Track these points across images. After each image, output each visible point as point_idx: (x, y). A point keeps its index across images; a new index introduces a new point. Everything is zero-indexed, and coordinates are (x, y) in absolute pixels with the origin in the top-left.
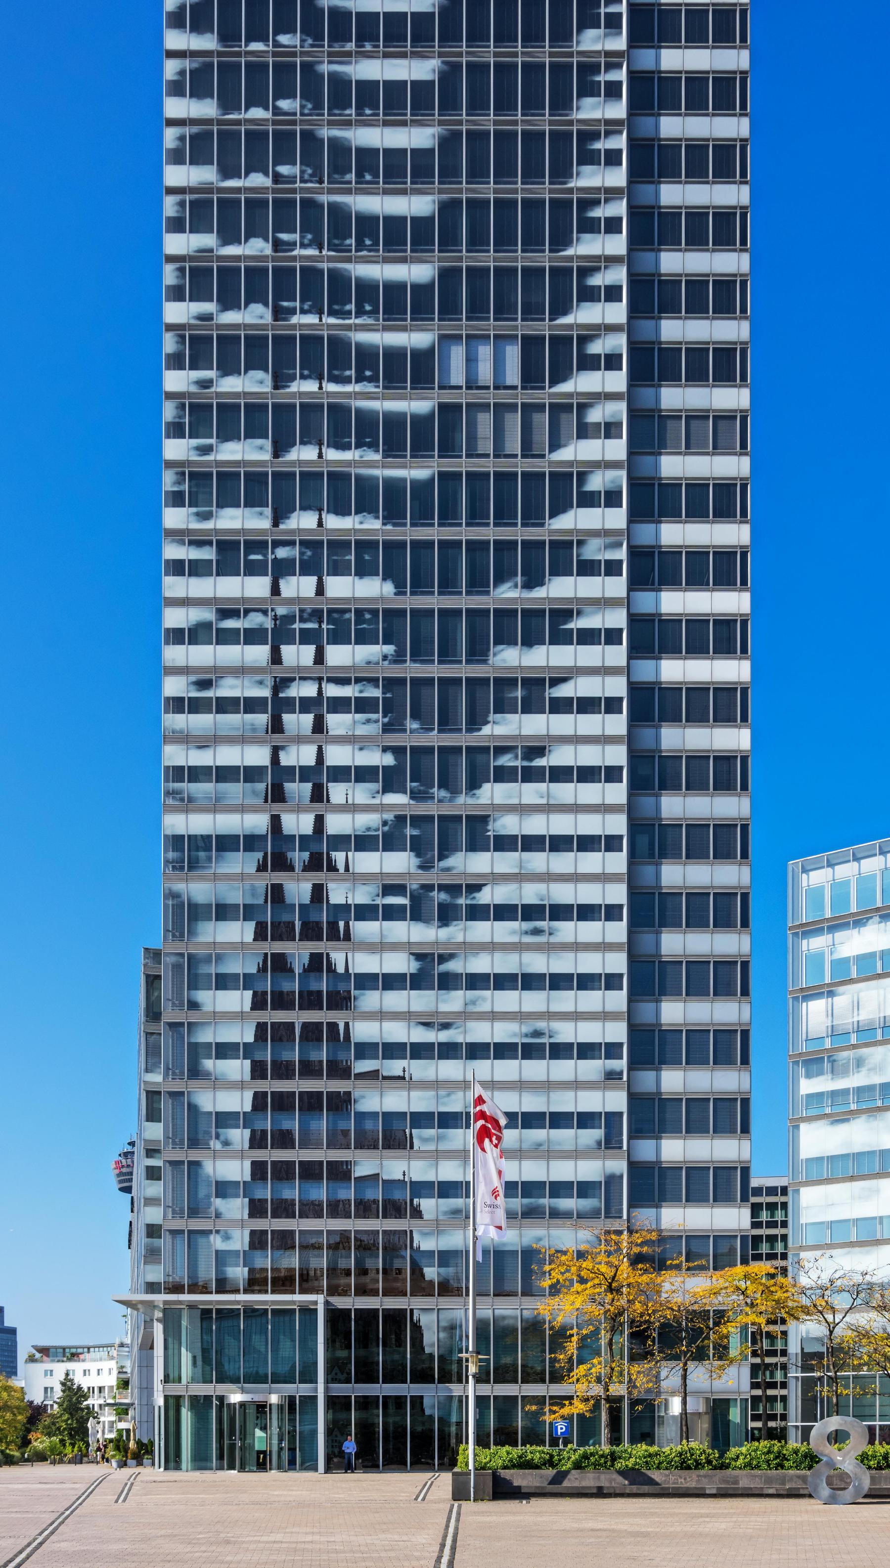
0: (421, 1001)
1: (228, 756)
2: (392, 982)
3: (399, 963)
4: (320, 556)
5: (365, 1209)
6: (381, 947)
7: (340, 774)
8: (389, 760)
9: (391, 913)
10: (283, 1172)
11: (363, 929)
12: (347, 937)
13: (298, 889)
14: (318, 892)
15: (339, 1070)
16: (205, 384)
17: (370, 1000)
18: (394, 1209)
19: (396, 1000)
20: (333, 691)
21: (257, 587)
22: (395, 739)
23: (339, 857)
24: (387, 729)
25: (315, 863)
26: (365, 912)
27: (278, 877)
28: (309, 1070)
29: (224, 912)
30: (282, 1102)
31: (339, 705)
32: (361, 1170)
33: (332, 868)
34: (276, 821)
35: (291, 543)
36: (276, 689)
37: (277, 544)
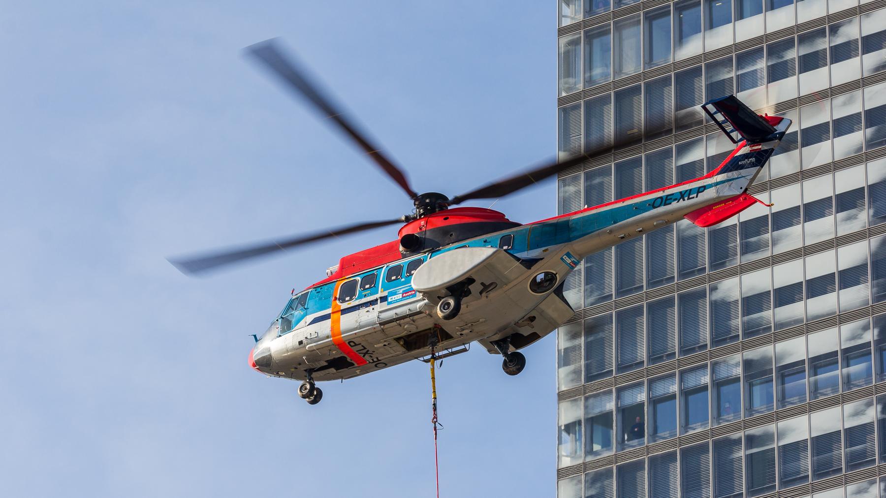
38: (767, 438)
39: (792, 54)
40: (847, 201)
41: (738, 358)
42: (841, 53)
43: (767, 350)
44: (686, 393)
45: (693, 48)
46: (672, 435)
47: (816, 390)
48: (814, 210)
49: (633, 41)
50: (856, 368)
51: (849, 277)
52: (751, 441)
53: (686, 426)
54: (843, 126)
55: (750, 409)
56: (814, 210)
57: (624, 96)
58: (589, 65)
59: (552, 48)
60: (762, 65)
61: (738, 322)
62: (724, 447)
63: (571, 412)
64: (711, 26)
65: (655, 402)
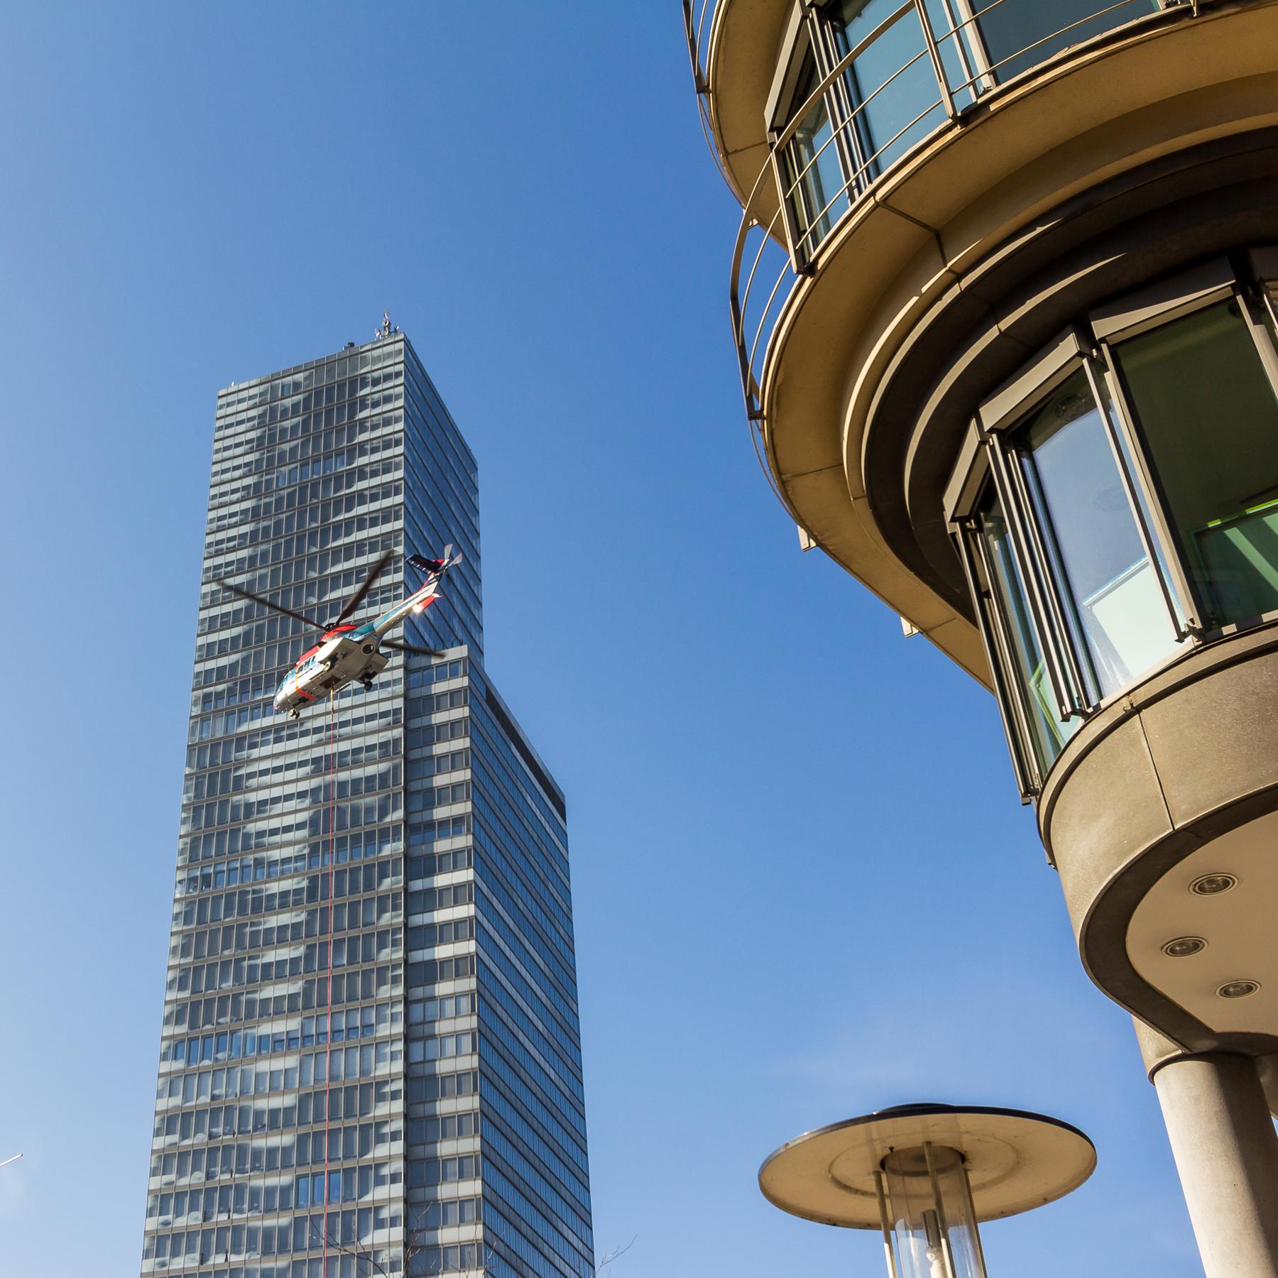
16: (166, 1223)
38: (261, 891)
39: (284, 733)
40: (302, 795)
41: (252, 857)
42: (304, 734)
43: (264, 854)
44: (230, 870)
45: (244, 728)
46: (223, 888)
47: (282, 872)
48: (288, 798)
49: (221, 723)
50: (299, 864)
51: (300, 826)
52: (254, 892)
53: (228, 884)
54: (302, 764)
55: (255, 878)
56: (288, 798)
57: (215, 746)
58: (201, 732)
59: (186, 725)
60: (272, 737)
61: (253, 842)
62: (243, 894)
63: (181, 875)
64: (252, 719)
65: (216, 873)
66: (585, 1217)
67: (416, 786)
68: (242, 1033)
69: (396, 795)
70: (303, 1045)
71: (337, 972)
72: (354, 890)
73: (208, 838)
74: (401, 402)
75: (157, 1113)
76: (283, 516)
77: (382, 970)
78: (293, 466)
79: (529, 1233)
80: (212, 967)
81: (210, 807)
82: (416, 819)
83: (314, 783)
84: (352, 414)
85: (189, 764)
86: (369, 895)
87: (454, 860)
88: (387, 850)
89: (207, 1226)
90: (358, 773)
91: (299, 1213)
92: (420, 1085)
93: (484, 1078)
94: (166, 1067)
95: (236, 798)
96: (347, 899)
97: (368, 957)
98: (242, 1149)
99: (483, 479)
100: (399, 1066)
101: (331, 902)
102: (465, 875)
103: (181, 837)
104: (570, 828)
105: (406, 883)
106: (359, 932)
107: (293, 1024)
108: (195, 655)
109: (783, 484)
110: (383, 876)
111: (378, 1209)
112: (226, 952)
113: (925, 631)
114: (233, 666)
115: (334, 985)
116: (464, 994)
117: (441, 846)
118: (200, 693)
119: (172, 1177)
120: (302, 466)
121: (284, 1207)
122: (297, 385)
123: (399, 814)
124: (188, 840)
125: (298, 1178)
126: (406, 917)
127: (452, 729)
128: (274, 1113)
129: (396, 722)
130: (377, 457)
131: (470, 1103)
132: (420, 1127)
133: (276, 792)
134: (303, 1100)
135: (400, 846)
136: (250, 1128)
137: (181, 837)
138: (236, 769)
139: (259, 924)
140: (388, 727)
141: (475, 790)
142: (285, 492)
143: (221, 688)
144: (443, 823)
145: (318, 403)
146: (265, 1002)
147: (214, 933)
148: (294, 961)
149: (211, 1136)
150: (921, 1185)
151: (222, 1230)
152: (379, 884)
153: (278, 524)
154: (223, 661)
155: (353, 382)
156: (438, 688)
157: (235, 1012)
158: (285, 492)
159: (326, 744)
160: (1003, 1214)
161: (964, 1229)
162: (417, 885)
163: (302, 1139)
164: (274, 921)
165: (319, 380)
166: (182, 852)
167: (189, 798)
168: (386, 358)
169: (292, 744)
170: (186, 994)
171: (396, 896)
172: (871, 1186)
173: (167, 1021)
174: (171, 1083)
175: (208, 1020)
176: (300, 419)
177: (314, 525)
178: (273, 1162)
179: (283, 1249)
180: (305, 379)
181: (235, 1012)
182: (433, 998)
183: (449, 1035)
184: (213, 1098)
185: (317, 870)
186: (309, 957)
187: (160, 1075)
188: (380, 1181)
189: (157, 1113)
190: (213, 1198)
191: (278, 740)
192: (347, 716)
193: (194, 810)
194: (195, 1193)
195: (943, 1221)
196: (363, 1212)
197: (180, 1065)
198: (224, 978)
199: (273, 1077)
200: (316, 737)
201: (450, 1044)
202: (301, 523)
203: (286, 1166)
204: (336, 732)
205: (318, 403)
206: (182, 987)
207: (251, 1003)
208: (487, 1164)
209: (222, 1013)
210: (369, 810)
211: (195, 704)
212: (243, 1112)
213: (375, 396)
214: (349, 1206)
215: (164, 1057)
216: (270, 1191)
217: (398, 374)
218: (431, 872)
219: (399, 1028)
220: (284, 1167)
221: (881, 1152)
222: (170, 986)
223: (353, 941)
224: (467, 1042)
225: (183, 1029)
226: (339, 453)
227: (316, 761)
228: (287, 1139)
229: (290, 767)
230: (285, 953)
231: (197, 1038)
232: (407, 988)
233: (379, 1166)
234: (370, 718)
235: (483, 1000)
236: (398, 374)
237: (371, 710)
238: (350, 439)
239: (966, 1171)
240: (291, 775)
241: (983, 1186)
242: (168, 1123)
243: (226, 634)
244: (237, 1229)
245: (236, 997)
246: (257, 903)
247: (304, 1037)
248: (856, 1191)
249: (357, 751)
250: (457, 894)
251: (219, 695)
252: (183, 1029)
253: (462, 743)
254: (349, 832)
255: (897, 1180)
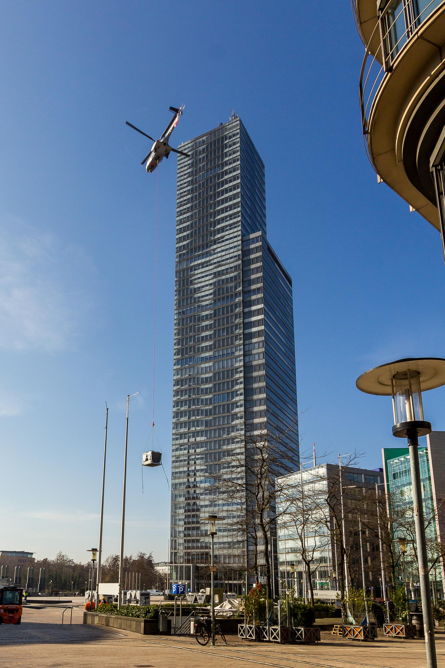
0: (211, 509)
1: (181, 469)
2: (206, 506)
3: (207, 503)
4: (196, 434)
5: (202, 548)
6: (204, 500)
7: (198, 471)
8: (206, 467)
9: (206, 494)
10: (189, 541)
11: (202, 497)
12: (199, 499)
13: (192, 491)
14: (195, 491)
15: (198, 522)
16: (178, 409)
17: (203, 509)
18: (207, 547)
19: (207, 509)
20: (197, 457)
21: (186, 441)
22: (206, 464)
23: (198, 485)
24: (206, 462)
25: (195, 486)
26: (202, 494)
27: (189, 489)
28: (193, 523)
29: (180, 496)
30: (189, 529)
31: (198, 459)
32: (201, 541)
33: (197, 487)
34: (188, 480)
35: (191, 433)
36: (188, 458)
37: (189, 433)
39: (205, 265)
40: (211, 284)
44: (190, 309)
45: (192, 264)
46: (189, 315)
47: (206, 309)
48: (207, 286)
49: (185, 263)
51: (211, 294)
52: (198, 315)
54: (211, 274)
55: (198, 311)
56: (207, 286)
57: (184, 271)
58: (179, 267)
59: (175, 264)
61: (197, 300)
62: (195, 316)
63: (176, 312)
64: (195, 261)
65: (186, 310)
66: (295, 402)
67: (246, 279)
68: (196, 357)
69: (239, 282)
70: (214, 359)
71: (223, 337)
72: (227, 312)
73: (183, 300)
74: (239, 145)
75: (174, 380)
76: (201, 191)
77: (236, 336)
78: (203, 172)
79: (279, 407)
80: (187, 338)
81: (183, 290)
82: (246, 289)
83: (214, 280)
84: (223, 151)
85: (176, 277)
86: (232, 314)
87: (257, 302)
88: (237, 300)
89: (190, 409)
90: (228, 276)
91: (215, 405)
92: (248, 368)
93: (267, 365)
94: (175, 367)
95: (191, 287)
96: (225, 316)
97: (232, 333)
98: (198, 389)
99: (267, 171)
100: (242, 363)
101: (221, 316)
102: (261, 306)
103: (175, 300)
104: (293, 289)
105: (243, 309)
106: (229, 325)
107: (211, 353)
108: (176, 241)
109: (373, 159)
110: (236, 308)
111: (237, 403)
112: (191, 334)
113: (417, 210)
114: (188, 244)
115: (222, 342)
116: (261, 342)
117: (254, 297)
118: (178, 254)
119: (179, 397)
120: (206, 172)
121: (211, 403)
122: (203, 141)
123: (241, 288)
124: (177, 301)
125: (214, 396)
126: (243, 320)
127: (257, 260)
128: (206, 378)
129: (239, 259)
130: (231, 166)
131: (262, 373)
132: (248, 380)
133: (203, 284)
134: (215, 374)
135: (241, 298)
136: (200, 383)
137: (175, 300)
138: (191, 278)
139: (200, 325)
140: (237, 261)
141: (264, 279)
142: (201, 182)
143: (184, 252)
144: (254, 290)
145: (211, 148)
146: (203, 347)
147: (187, 328)
148: (211, 335)
149: (189, 386)
150: (406, 382)
151: (194, 410)
152: (235, 310)
153: (200, 194)
154: (185, 243)
155: (222, 138)
156: (252, 246)
157: (194, 351)
158: (201, 182)
159: (218, 267)
160: (429, 389)
161: (417, 394)
162: (246, 310)
163: (215, 385)
164: (204, 324)
165: (211, 139)
166: (176, 305)
167: (177, 288)
168: (233, 128)
169: (207, 268)
170: (180, 347)
171: (240, 314)
172: (390, 383)
173: (175, 355)
174: (177, 372)
175: (186, 354)
176: (205, 154)
177: (211, 193)
178: (207, 391)
179: (211, 414)
180: (206, 138)
181: (194, 351)
182: (252, 343)
183: (256, 354)
184: (189, 375)
185: (216, 307)
186: (215, 333)
187: (174, 370)
188: (237, 395)
189: (174, 380)
190: (190, 402)
191: (203, 268)
192: (224, 258)
193: (178, 291)
194: (186, 401)
195: (411, 391)
196: (233, 404)
197: (179, 367)
198: (190, 341)
199: (206, 368)
200: (214, 266)
201: (257, 357)
202: (207, 193)
203: (211, 392)
204: (220, 263)
205: (211, 148)
206: (178, 345)
207: (198, 348)
208: (268, 389)
209: (190, 352)
210: (231, 288)
211: (177, 258)
212: (198, 378)
213: (230, 143)
214: (229, 402)
215: (175, 365)
216: (206, 399)
217: (237, 134)
218: (250, 306)
219: (242, 353)
220: (210, 393)
221: (394, 373)
222: (175, 344)
223: (228, 328)
224: (261, 356)
225: (179, 356)
226: (219, 166)
227: (215, 273)
228: (211, 385)
229: (207, 276)
230: (207, 333)
231: (183, 359)
232: (244, 341)
233: (237, 391)
234: (231, 258)
235: (266, 343)
236: (237, 134)
237: (231, 255)
238: (222, 160)
239: (419, 377)
240: (207, 278)
241: (424, 381)
242: (177, 383)
243: (185, 234)
244: (198, 410)
245: (194, 346)
246: (199, 318)
247: (214, 357)
248: (385, 385)
249: (227, 269)
250: (258, 312)
251: (184, 254)
252: (179, 356)
253: (259, 264)
254: (225, 295)
255: (398, 381)
